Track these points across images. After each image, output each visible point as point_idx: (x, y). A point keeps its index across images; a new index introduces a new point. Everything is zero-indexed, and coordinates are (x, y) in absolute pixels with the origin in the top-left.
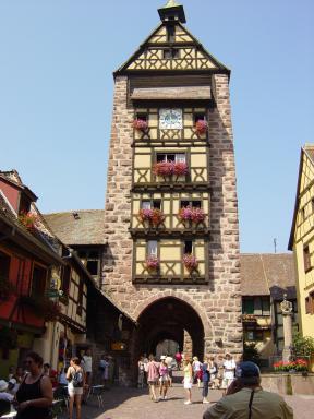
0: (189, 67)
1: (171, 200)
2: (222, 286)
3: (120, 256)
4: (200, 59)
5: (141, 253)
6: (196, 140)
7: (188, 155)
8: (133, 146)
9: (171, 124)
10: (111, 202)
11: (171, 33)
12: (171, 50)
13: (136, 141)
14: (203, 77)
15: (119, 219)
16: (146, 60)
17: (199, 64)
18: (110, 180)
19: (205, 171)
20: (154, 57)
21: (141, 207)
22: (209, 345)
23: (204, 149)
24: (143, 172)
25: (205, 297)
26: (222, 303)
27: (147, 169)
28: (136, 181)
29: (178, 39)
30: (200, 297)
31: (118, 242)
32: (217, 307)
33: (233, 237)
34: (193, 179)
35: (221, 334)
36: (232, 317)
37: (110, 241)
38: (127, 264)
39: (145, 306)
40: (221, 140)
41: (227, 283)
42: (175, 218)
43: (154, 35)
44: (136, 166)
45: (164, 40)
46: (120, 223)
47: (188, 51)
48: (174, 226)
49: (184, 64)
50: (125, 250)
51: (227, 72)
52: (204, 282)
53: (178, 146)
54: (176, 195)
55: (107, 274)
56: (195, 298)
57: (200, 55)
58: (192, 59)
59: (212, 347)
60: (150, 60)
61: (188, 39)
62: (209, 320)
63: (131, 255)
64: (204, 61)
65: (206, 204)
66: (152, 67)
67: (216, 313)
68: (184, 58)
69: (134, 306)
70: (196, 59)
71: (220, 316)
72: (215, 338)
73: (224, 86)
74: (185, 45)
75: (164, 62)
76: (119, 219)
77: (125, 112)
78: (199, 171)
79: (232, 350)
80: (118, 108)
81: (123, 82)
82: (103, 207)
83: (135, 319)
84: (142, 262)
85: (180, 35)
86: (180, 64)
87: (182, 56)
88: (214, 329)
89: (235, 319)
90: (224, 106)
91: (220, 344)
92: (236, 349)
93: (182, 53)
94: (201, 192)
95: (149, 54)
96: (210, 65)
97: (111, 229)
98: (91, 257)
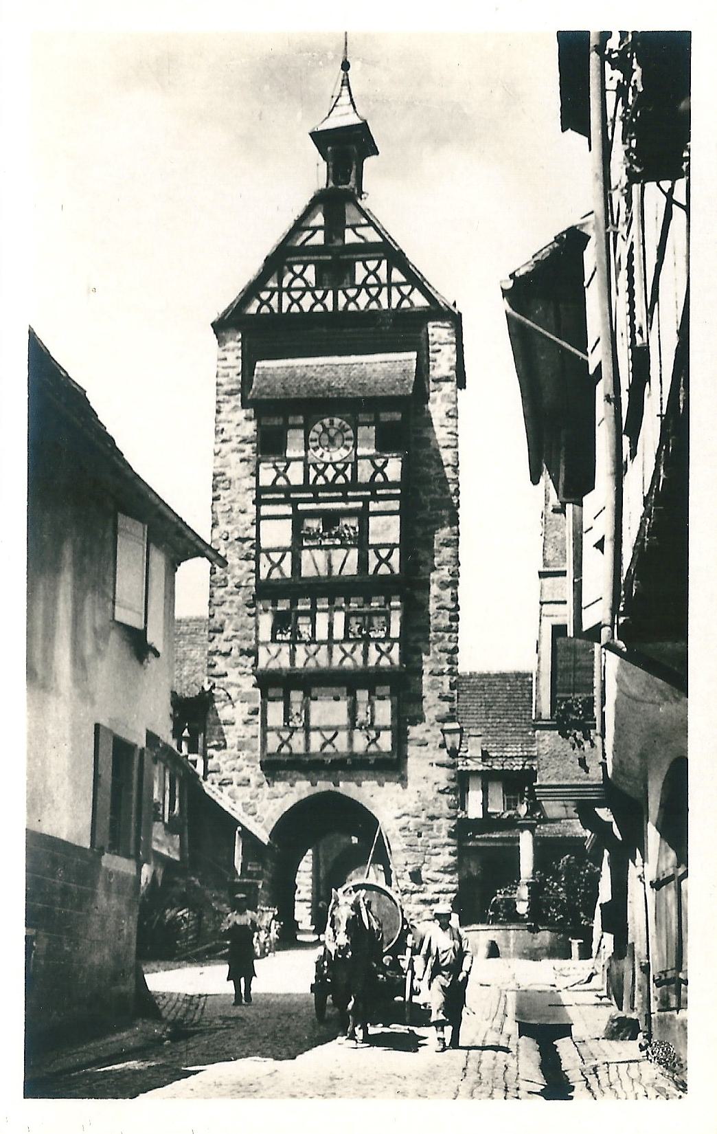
1: (330, 612)
4: (398, 285)
7: (363, 516)
8: (258, 502)
11: (335, 226)
12: (336, 266)
13: (260, 490)
14: (404, 330)
17: (396, 297)
19: (396, 552)
20: (299, 283)
23: (395, 505)
24: (276, 557)
27: (284, 550)
29: (350, 237)
34: (371, 571)
36: (439, 829)
42: (336, 647)
43: (299, 226)
45: (319, 239)
47: (372, 265)
50: (246, 707)
51: (455, 320)
53: (345, 499)
54: (340, 601)
57: (397, 276)
58: (380, 286)
60: (289, 289)
61: (372, 236)
63: (258, 718)
64: (406, 289)
66: (295, 309)
68: (365, 285)
75: (319, 294)
78: (384, 553)
80: (226, 408)
82: (205, 613)
84: (278, 730)
87: (359, 281)
89: (444, 833)
93: (360, 273)
96: (419, 300)
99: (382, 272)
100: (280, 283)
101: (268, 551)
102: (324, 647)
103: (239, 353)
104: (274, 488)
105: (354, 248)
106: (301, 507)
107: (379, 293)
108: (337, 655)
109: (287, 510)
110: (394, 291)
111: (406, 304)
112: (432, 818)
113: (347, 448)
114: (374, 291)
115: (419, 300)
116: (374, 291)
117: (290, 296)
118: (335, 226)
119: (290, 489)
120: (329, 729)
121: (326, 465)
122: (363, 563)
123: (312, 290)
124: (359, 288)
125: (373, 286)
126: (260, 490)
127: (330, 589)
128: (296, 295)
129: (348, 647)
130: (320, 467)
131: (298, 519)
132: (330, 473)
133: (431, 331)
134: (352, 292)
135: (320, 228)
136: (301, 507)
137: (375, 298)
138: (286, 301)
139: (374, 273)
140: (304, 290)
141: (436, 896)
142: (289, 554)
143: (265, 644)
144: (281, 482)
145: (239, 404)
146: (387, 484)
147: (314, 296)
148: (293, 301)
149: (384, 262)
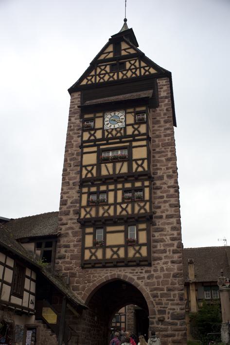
0: (134, 76)
1: (115, 190)
2: (165, 267)
3: (72, 244)
4: (144, 67)
5: (89, 241)
6: (137, 135)
7: (130, 148)
8: (82, 147)
9: (115, 122)
10: (65, 198)
11: (117, 49)
13: (83, 142)
15: (72, 212)
16: (95, 75)
17: (143, 71)
18: (64, 179)
19: (146, 161)
20: (103, 72)
21: (88, 197)
22: (153, 323)
23: (144, 143)
24: (89, 168)
25: (149, 278)
26: (164, 283)
27: (93, 165)
28: (84, 177)
29: (123, 53)
30: (143, 278)
31: (70, 232)
32: (161, 286)
33: (174, 220)
35: (163, 312)
37: (62, 232)
38: (76, 251)
39: (93, 289)
40: (162, 134)
41: (169, 264)
42: (118, 206)
43: (102, 52)
44: (84, 163)
45: (111, 55)
46: (71, 215)
47: (132, 62)
48: (118, 213)
49: (129, 74)
51: (167, 75)
52: (145, 262)
53: (121, 142)
54: (120, 186)
55: (60, 261)
56: (138, 278)
57: (143, 64)
58: (136, 69)
59: (155, 325)
62: (152, 299)
65: (147, 190)
67: (159, 293)
68: (130, 69)
69: (83, 289)
70: (140, 68)
71: (162, 295)
72: (158, 316)
73: (165, 88)
74: (130, 57)
75: (111, 74)
76: (72, 212)
77: (78, 121)
78: (140, 162)
79: (174, 327)
80: (73, 119)
81: (77, 95)
83: (83, 302)
84: (90, 248)
85: (125, 50)
86: (125, 75)
88: (157, 308)
90: (165, 105)
91: (161, 321)
92: (179, 327)
93: (128, 65)
94: (143, 181)
95: (98, 70)
96: (152, 71)
97: (64, 221)
98: (45, 247)
99: (137, 64)
100: (96, 72)
101: (86, 166)
102: (112, 208)
103: (79, 100)
104: (89, 141)
105: (126, 57)
106: (101, 147)
107: (136, 71)
108: (119, 209)
109: (95, 149)
110: (142, 69)
111: (147, 73)
112: (169, 290)
113: (121, 122)
114: (134, 71)
115: (152, 71)
116: (134, 71)
117: (100, 77)
118: (117, 49)
119: (96, 140)
120: (115, 246)
121: (113, 129)
122: (130, 167)
123: (108, 74)
124: (128, 70)
125: (133, 69)
126: (83, 142)
127: (115, 179)
128: (102, 76)
129: (124, 206)
130: (110, 131)
131: (99, 152)
132: (114, 133)
133: (158, 81)
134: (125, 72)
135: (111, 52)
136: (101, 147)
137: (134, 73)
138: (98, 78)
139: (133, 64)
140: (105, 74)
141: (173, 332)
142: (95, 167)
143: (84, 207)
144: (92, 138)
145: (79, 117)
146: (140, 134)
147: (109, 75)
148: (101, 78)
149: (138, 61)
